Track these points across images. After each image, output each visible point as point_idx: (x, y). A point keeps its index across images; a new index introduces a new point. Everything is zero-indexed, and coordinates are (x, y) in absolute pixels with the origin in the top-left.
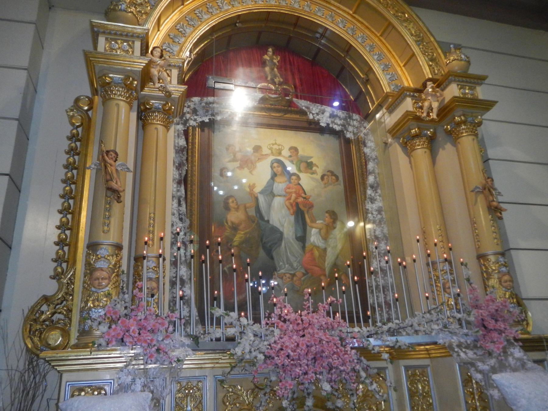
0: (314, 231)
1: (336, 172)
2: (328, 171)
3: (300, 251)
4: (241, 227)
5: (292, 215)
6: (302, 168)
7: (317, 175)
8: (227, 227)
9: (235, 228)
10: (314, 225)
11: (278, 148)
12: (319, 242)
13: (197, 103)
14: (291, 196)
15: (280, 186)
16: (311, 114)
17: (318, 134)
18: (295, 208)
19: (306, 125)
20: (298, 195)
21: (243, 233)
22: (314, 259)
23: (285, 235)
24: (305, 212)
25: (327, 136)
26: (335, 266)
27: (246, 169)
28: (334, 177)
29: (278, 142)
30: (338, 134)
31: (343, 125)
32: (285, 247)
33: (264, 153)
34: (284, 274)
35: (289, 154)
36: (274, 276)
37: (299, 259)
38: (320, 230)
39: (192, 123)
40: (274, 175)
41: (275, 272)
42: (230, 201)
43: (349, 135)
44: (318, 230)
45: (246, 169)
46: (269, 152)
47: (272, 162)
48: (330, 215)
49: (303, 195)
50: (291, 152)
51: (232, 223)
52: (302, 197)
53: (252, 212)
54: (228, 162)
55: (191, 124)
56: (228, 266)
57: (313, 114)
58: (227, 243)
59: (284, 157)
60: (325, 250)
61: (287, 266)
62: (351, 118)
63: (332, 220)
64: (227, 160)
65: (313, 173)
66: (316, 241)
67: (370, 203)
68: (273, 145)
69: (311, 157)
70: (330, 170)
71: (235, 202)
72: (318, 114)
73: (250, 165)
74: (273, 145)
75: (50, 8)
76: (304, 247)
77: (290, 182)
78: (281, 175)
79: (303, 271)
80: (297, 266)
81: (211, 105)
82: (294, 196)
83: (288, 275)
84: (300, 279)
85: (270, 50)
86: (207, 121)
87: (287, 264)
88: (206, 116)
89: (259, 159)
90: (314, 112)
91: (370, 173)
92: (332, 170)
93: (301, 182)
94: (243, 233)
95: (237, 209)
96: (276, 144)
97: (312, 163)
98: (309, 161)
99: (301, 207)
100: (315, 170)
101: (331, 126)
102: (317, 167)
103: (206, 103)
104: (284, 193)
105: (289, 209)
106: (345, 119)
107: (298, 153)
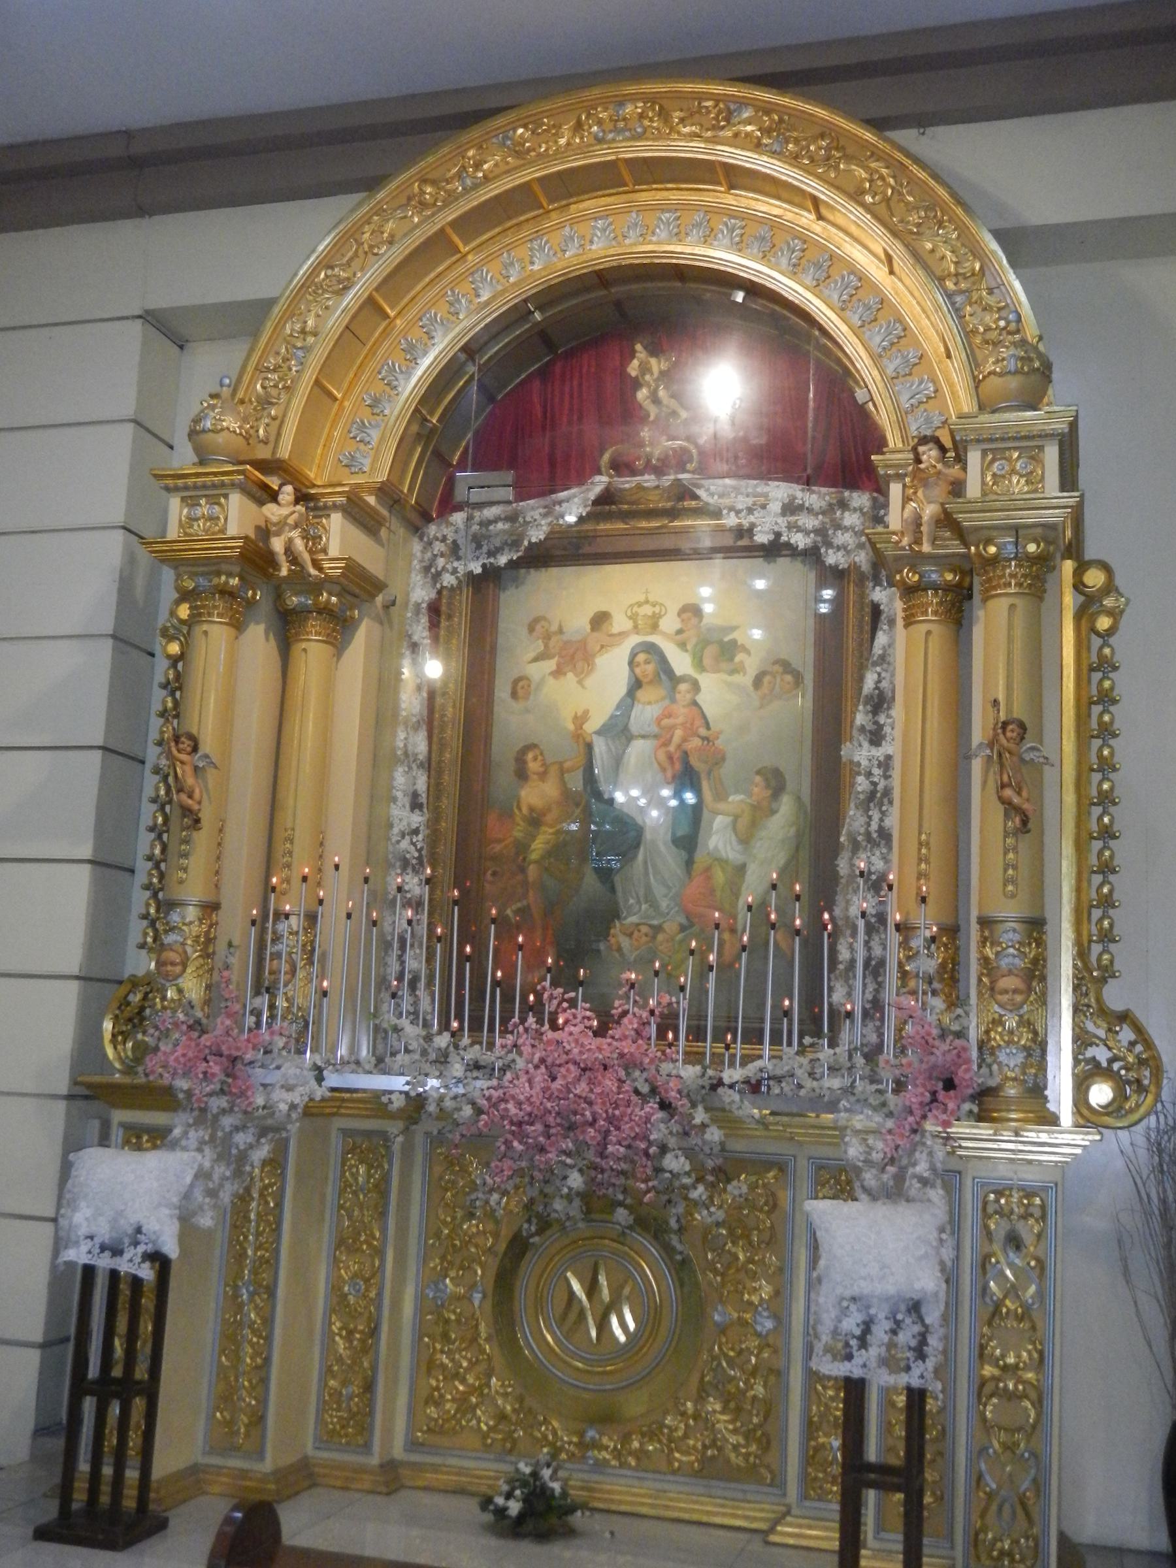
0: (720, 822)
1: (796, 663)
2: (776, 662)
3: (680, 872)
4: (549, 818)
5: (668, 783)
6: (707, 661)
7: (745, 674)
8: (518, 819)
9: (535, 821)
10: (721, 806)
11: (650, 614)
12: (729, 848)
13: (461, 526)
14: (672, 737)
15: (645, 713)
16: (732, 514)
17: (761, 559)
18: (678, 766)
19: (728, 541)
20: (691, 732)
21: (551, 831)
22: (712, 891)
23: (648, 836)
24: (703, 776)
25: (783, 562)
26: (758, 910)
27: (570, 675)
28: (789, 678)
29: (651, 599)
30: (812, 555)
31: (820, 531)
32: (645, 862)
33: (615, 629)
34: (638, 925)
35: (677, 625)
36: (612, 931)
37: (674, 891)
38: (736, 818)
39: (448, 580)
40: (636, 685)
41: (617, 922)
42: (530, 756)
43: (832, 558)
44: (731, 818)
45: (570, 675)
46: (628, 625)
47: (633, 649)
48: (767, 780)
49: (703, 732)
50: (683, 621)
51: (531, 809)
52: (699, 736)
53: (576, 783)
54: (530, 662)
55: (445, 584)
56: (514, 907)
57: (738, 512)
58: (517, 854)
59: (664, 634)
60: (741, 869)
61: (644, 907)
62: (843, 505)
63: (769, 792)
64: (532, 655)
65: (732, 672)
66: (721, 846)
67: (866, 744)
68: (640, 604)
69: (733, 629)
70: (782, 657)
71: (540, 758)
72: (750, 511)
73: (580, 665)
74: (640, 604)
75: (181, 347)
76: (689, 863)
77: (673, 700)
78: (651, 682)
79: (683, 920)
80: (668, 906)
81: (491, 527)
82: (678, 734)
83: (644, 929)
84: (672, 939)
85: (638, 347)
86: (478, 570)
87: (646, 902)
88: (478, 558)
89: (602, 647)
90: (740, 506)
91: (875, 664)
92: (786, 657)
93: (700, 699)
94: (551, 831)
95: (543, 776)
96: (647, 602)
97: (734, 642)
98: (726, 639)
99: (694, 761)
100: (742, 662)
101: (784, 538)
102: (748, 653)
103: (481, 524)
104: (655, 729)
105: (664, 770)
106: (829, 510)
107: (701, 621)
